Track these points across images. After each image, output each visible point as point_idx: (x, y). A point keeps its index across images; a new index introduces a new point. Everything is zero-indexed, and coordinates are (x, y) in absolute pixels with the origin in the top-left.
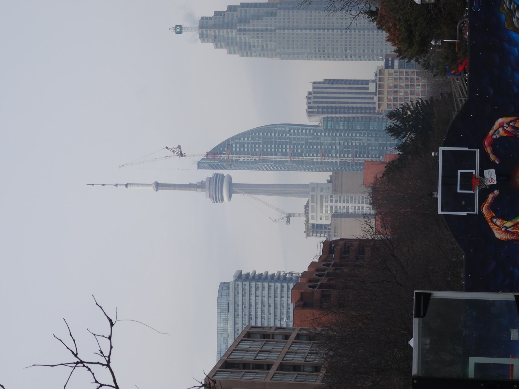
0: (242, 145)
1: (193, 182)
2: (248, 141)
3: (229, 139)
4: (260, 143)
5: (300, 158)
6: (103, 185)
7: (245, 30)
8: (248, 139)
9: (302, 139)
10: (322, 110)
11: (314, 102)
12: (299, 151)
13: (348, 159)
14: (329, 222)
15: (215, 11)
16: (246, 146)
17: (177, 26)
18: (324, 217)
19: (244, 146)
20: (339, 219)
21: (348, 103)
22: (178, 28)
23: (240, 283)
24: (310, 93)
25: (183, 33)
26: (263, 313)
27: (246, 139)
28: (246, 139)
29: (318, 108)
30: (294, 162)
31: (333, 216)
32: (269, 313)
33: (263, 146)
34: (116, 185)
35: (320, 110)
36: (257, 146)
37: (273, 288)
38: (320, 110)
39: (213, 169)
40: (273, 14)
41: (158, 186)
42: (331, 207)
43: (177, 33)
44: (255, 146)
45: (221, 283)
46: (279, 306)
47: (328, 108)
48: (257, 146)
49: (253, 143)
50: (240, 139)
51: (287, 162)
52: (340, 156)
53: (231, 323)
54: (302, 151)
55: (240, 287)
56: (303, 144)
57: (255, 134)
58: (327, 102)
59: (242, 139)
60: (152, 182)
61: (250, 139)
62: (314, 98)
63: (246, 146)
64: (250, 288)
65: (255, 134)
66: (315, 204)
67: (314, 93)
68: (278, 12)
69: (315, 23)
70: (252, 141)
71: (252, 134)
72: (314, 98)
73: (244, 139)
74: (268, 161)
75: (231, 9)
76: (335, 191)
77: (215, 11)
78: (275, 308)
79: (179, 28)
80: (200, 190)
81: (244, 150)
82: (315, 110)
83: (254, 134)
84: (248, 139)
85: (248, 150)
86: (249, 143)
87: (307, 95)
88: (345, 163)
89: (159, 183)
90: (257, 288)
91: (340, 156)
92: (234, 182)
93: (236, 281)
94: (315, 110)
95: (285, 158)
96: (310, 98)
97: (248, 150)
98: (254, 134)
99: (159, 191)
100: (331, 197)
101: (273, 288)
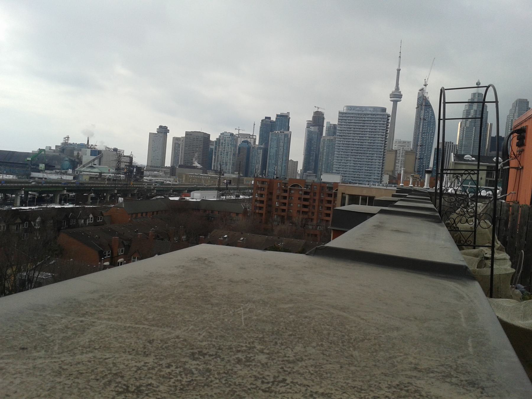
0: (428, 112)
1: (399, 85)
4: (428, 119)
5: (420, 136)
7: (476, 113)
9: (428, 138)
11: (448, 145)
12: (423, 136)
13: (418, 157)
14: (393, 149)
18: (395, 146)
20: (395, 153)
21: (447, 159)
23: (386, 117)
24: (452, 143)
26: (372, 126)
30: (419, 133)
31: (396, 151)
32: (372, 129)
33: (427, 121)
34: (400, 52)
37: (383, 131)
39: (418, 99)
41: (399, 70)
42: (400, 150)
45: (386, 108)
46: (375, 133)
51: (419, 131)
52: (419, 153)
53: (369, 112)
54: (423, 137)
55: (385, 117)
56: (426, 137)
58: (448, 150)
60: (401, 68)
62: (451, 145)
64: (384, 121)
66: (402, 143)
67: (453, 145)
72: (451, 145)
74: (420, 123)
76: (407, 152)
78: (374, 132)
80: (396, 88)
87: (452, 142)
88: (416, 155)
89: (400, 71)
90: (383, 124)
91: (419, 153)
92: (398, 102)
93: (387, 115)
95: (421, 130)
96: (450, 143)
99: (397, 71)
100: (405, 150)
101: (383, 131)
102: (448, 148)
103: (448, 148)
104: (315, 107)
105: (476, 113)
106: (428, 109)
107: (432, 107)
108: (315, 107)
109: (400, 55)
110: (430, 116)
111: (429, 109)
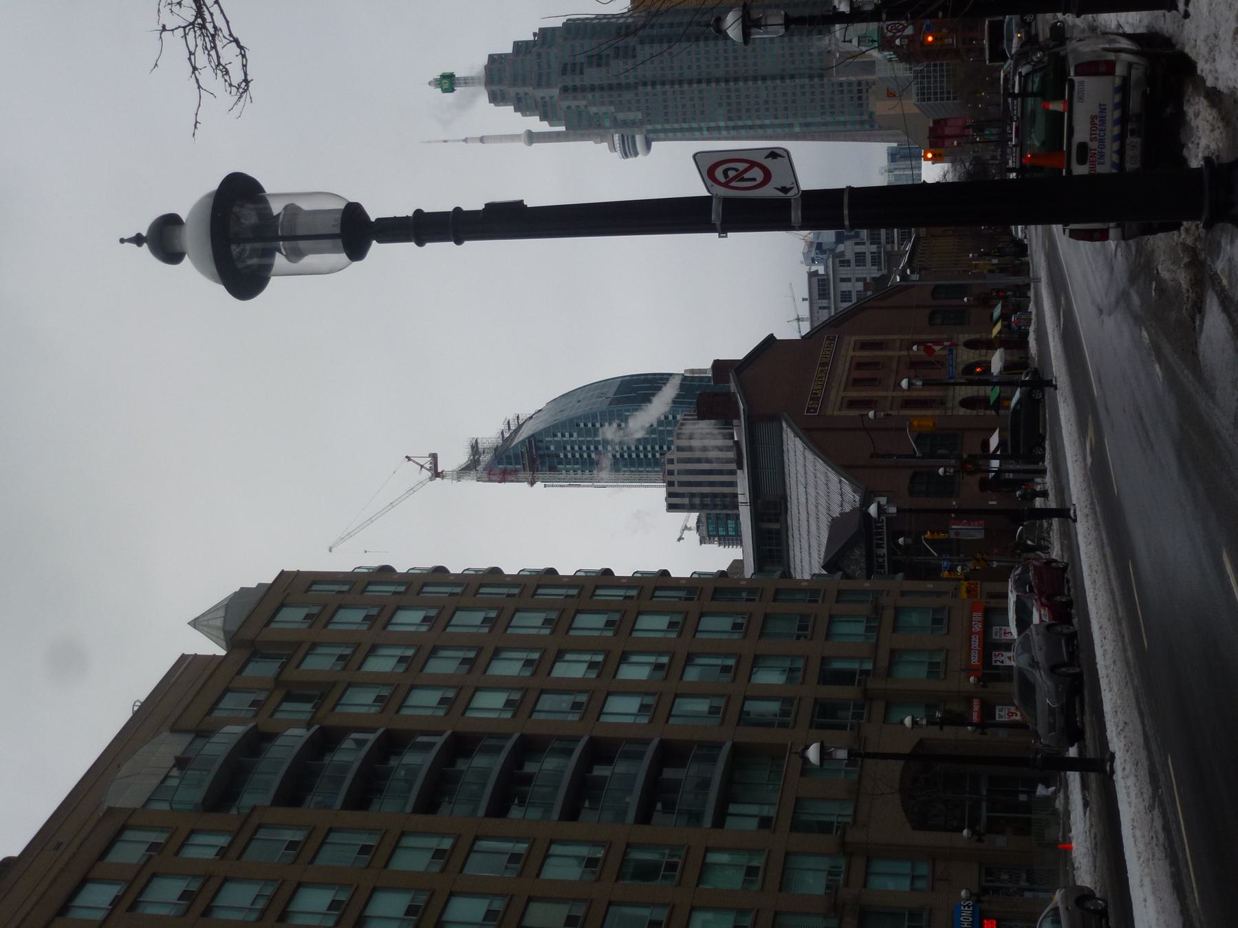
2: (572, 439)
3: (533, 436)
6: (445, 141)
7: (575, 89)
8: (571, 435)
10: (701, 502)
11: (681, 484)
15: (514, 42)
16: (569, 448)
17: (444, 76)
19: (565, 448)
22: (443, 81)
25: (458, 89)
27: (567, 435)
28: (567, 435)
29: (692, 495)
34: (465, 140)
35: (697, 501)
36: (592, 448)
38: (697, 501)
40: (629, 53)
43: (445, 91)
44: (588, 448)
47: (715, 495)
48: (592, 448)
49: (582, 442)
50: (555, 435)
57: (586, 425)
58: (712, 484)
59: (559, 435)
61: (575, 435)
62: (680, 472)
63: (569, 448)
65: (586, 425)
68: (639, 47)
69: (717, 66)
70: (580, 439)
71: (578, 425)
73: (563, 436)
75: (545, 34)
77: (514, 42)
79: (446, 81)
81: (566, 456)
82: (686, 501)
83: (582, 425)
84: (571, 435)
85: (573, 456)
86: (574, 442)
89: (534, 130)
94: (686, 501)
97: (573, 456)
98: (582, 425)
102: (700, 484)
103: (700, 484)
104: (680, 539)
105: (575, 89)
106: (548, 448)
107: (540, 433)
108: (680, 539)
109: (473, 140)
110: (579, 435)
111: (550, 441)
